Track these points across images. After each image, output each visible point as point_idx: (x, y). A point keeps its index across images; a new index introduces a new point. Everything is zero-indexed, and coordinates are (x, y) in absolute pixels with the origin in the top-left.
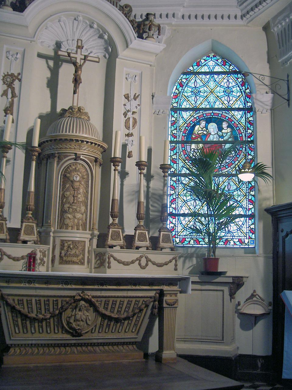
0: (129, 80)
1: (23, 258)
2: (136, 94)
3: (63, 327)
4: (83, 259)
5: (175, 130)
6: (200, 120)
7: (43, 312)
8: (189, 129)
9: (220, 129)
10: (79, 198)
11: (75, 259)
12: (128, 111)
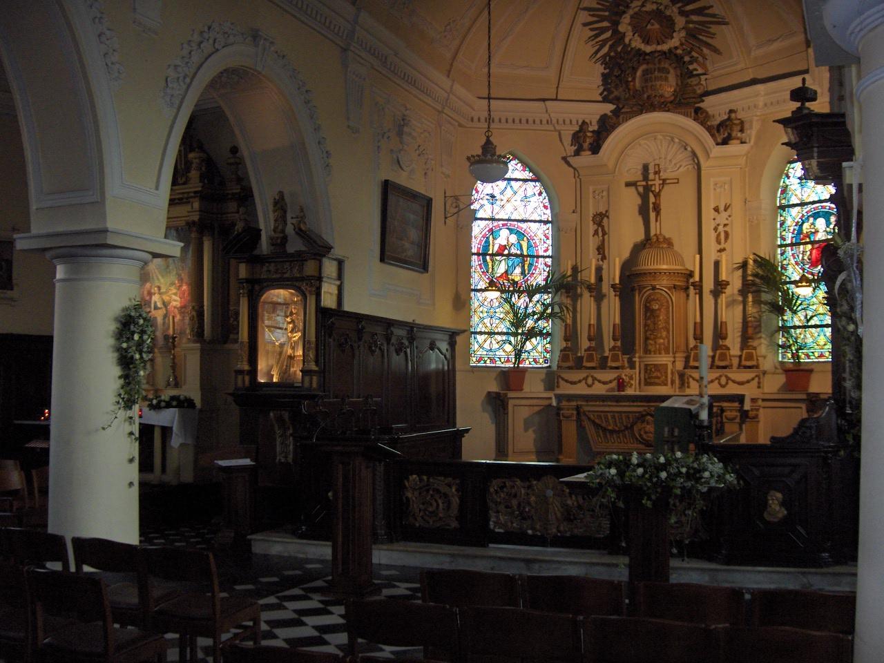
0: (718, 190)
1: (611, 382)
2: (726, 204)
3: (637, 439)
4: (667, 380)
7: (618, 424)
11: (657, 381)
12: (718, 225)
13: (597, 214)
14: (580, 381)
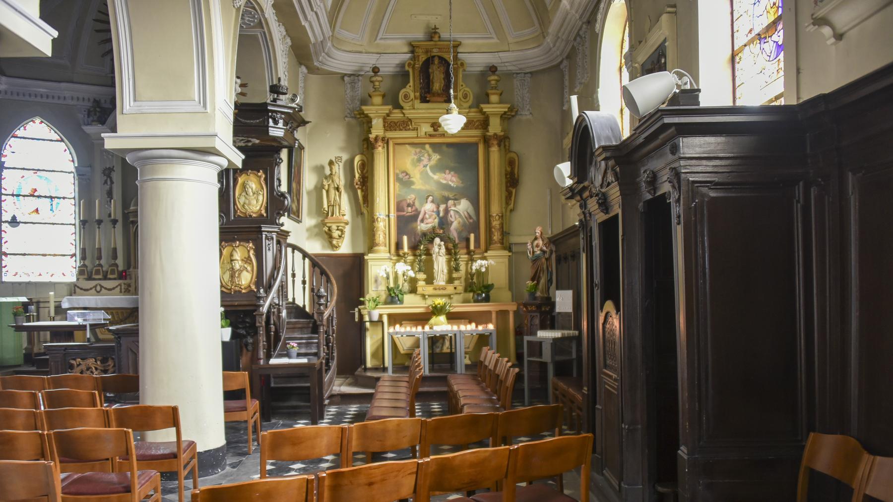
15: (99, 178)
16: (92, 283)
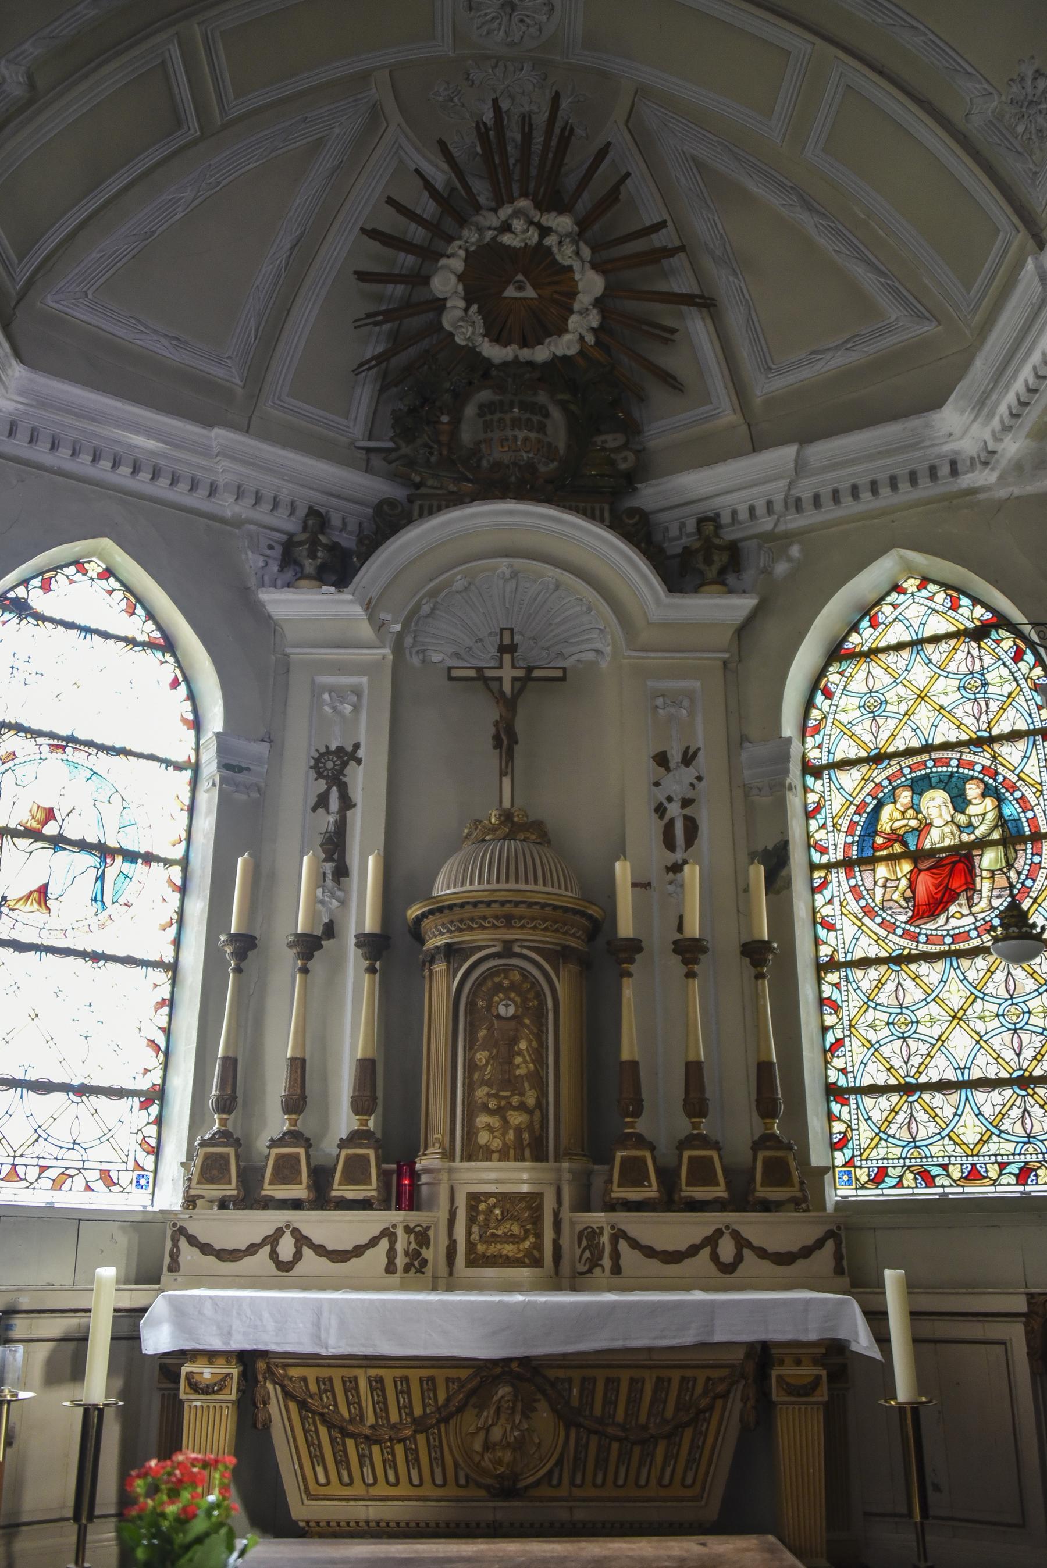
4: (539, 1246)
5: (820, 828)
6: (894, 789)
8: (863, 819)
9: (960, 802)
10: (518, 1067)
13: (328, 752)
14: (252, 1249)
15: (297, 785)
16: (257, 1224)
